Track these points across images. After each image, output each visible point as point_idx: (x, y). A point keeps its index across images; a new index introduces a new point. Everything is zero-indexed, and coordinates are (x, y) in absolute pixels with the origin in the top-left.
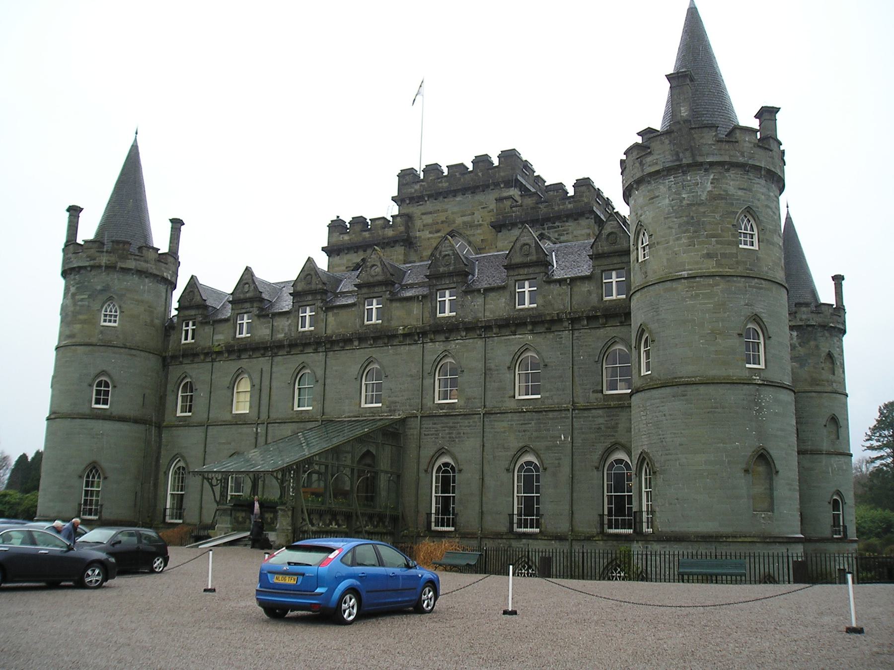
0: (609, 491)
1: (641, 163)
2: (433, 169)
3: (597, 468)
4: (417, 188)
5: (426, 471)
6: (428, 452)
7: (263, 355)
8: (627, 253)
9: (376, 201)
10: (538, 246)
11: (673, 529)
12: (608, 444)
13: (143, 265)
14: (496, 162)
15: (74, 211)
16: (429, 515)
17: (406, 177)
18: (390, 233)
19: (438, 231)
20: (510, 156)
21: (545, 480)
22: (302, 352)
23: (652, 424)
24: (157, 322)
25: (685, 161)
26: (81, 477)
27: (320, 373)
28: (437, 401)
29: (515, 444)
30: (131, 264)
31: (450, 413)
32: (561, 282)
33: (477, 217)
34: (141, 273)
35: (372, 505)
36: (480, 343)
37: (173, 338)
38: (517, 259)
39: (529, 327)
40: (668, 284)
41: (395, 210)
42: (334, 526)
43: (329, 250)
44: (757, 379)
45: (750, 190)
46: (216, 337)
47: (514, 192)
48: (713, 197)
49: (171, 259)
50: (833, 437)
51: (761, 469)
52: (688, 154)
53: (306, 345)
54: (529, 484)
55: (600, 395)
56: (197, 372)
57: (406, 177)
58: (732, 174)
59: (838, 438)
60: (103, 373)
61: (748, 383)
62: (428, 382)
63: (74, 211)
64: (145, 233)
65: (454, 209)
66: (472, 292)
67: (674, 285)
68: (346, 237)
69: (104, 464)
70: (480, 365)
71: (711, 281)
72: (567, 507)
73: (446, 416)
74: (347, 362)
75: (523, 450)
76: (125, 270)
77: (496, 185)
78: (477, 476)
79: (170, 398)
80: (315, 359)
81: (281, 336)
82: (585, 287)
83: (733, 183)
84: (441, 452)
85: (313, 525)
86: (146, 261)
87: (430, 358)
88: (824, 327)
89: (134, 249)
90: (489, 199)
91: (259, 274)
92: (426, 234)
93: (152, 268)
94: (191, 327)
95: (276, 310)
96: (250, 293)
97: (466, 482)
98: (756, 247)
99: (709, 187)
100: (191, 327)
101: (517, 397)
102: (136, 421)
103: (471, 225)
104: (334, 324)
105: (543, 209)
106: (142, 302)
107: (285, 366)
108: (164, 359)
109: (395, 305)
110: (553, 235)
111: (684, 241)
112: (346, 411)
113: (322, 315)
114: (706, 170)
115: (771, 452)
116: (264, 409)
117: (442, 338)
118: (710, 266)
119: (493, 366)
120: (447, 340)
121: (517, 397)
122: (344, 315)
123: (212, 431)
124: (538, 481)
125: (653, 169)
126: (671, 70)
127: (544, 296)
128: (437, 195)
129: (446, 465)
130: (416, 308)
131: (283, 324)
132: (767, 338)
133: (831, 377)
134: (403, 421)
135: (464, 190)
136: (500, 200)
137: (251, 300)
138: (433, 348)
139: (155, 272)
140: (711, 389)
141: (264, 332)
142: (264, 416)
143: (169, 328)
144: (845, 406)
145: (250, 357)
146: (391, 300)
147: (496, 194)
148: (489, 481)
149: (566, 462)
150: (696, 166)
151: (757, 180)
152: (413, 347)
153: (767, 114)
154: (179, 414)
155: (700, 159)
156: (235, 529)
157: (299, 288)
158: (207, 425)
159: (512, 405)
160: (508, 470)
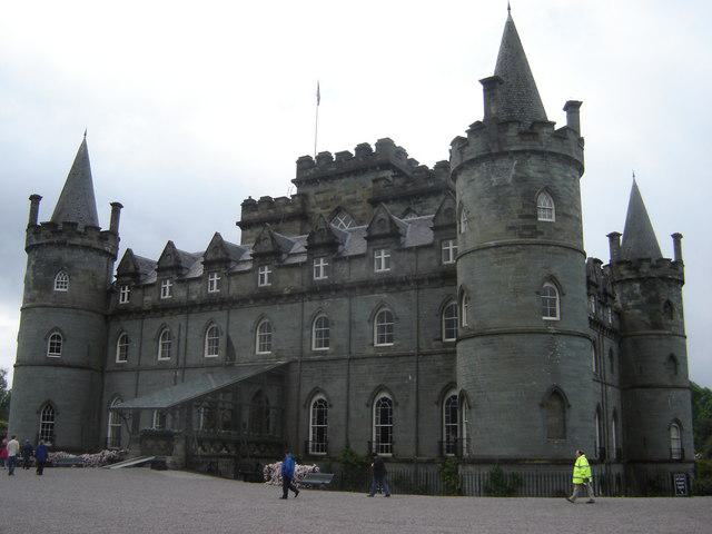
0: (447, 422)
1: (461, 153)
2: (325, 156)
3: (437, 403)
4: (314, 171)
5: (305, 406)
6: (307, 389)
7: (181, 313)
8: (454, 226)
9: (280, 184)
10: (392, 221)
11: (485, 453)
12: (445, 383)
14: (374, 148)
15: (35, 199)
16: (307, 442)
17: (304, 163)
18: (289, 210)
19: (328, 207)
20: (385, 144)
21: (397, 414)
22: (210, 310)
23: (470, 364)
24: (99, 287)
25: (493, 151)
26: (38, 413)
27: (223, 326)
28: (314, 349)
29: (373, 383)
30: (78, 241)
31: (323, 360)
32: (409, 250)
33: (358, 195)
35: (247, 436)
36: (346, 301)
37: (113, 298)
38: (376, 232)
39: (384, 287)
40: (480, 253)
41: (294, 190)
42: (224, 452)
43: (243, 225)
44: (552, 329)
45: (548, 172)
46: (146, 298)
47: (388, 174)
48: (518, 180)
49: (110, 237)
50: (672, 372)
51: (556, 403)
52: (496, 145)
53: (215, 304)
54: (385, 416)
55: (439, 343)
56: (131, 326)
57: (304, 163)
58: (533, 159)
59: (676, 374)
60: (52, 331)
61: (546, 332)
62: (307, 333)
63: (35, 199)
64: (93, 215)
65: (342, 189)
66: (341, 259)
67: (485, 252)
68: (256, 214)
69: (58, 403)
70: (346, 320)
71: (514, 249)
72: (414, 435)
73: (320, 361)
74: (243, 320)
75: (380, 389)
76: (71, 245)
77: (374, 168)
78: (344, 410)
79: (111, 348)
80: (219, 317)
81: (194, 297)
82: (426, 255)
83: (533, 168)
84: (316, 391)
85: (205, 451)
86: (92, 239)
87: (308, 313)
88: (663, 278)
89: (80, 229)
90: (368, 180)
91: (179, 247)
92: (318, 210)
93: (95, 243)
94: (127, 290)
95: (191, 276)
96: (173, 261)
97: (336, 413)
98: (553, 220)
99: (513, 172)
100: (127, 290)
101: (376, 345)
102: (81, 368)
103: (353, 202)
104: (235, 288)
105: (410, 187)
106: (87, 271)
107: (197, 322)
108: (106, 317)
109: (282, 271)
110: (418, 209)
111: (494, 216)
113: (225, 279)
114: (511, 158)
115: (565, 389)
116: (182, 356)
117: (317, 297)
119: (356, 320)
120: (321, 299)
121: (376, 345)
122: (242, 280)
123: (143, 375)
124: (391, 414)
125: (471, 157)
126: (490, 72)
127: (396, 263)
128: (326, 178)
129: (321, 401)
130: (297, 275)
131: (196, 287)
132: (562, 294)
133: (669, 322)
134: (287, 366)
135: (348, 173)
136: (375, 181)
137: (171, 268)
138: (311, 306)
139: (97, 246)
140: (513, 339)
141: (181, 294)
142: (181, 361)
143: (110, 292)
144: (684, 347)
145: (171, 314)
146: (279, 267)
147: (372, 176)
148: (353, 414)
149: (413, 398)
150: (503, 154)
151: (557, 164)
152: (297, 305)
153: (572, 108)
154: (118, 361)
155: (505, 149)
156: (143, 454)
157: (210, 257)
158: (137, 370)
159: (371, 352)
160: (368, 406)
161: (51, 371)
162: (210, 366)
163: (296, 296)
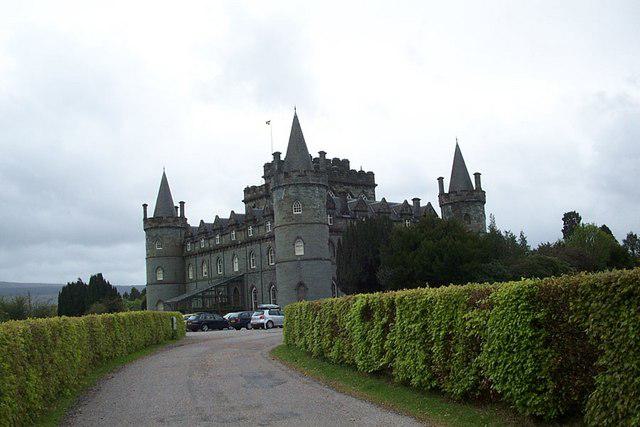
13: (168, 224)
15: (145, 206)
34: (169, 227)
56: (192, 260)
63: (145, 206)
76: (162, 227)
112: (229, 273)
118: (285, 222)
131: (212, 241)
161: (159, 287)
162: (220, 277)
163: (244, 244)
